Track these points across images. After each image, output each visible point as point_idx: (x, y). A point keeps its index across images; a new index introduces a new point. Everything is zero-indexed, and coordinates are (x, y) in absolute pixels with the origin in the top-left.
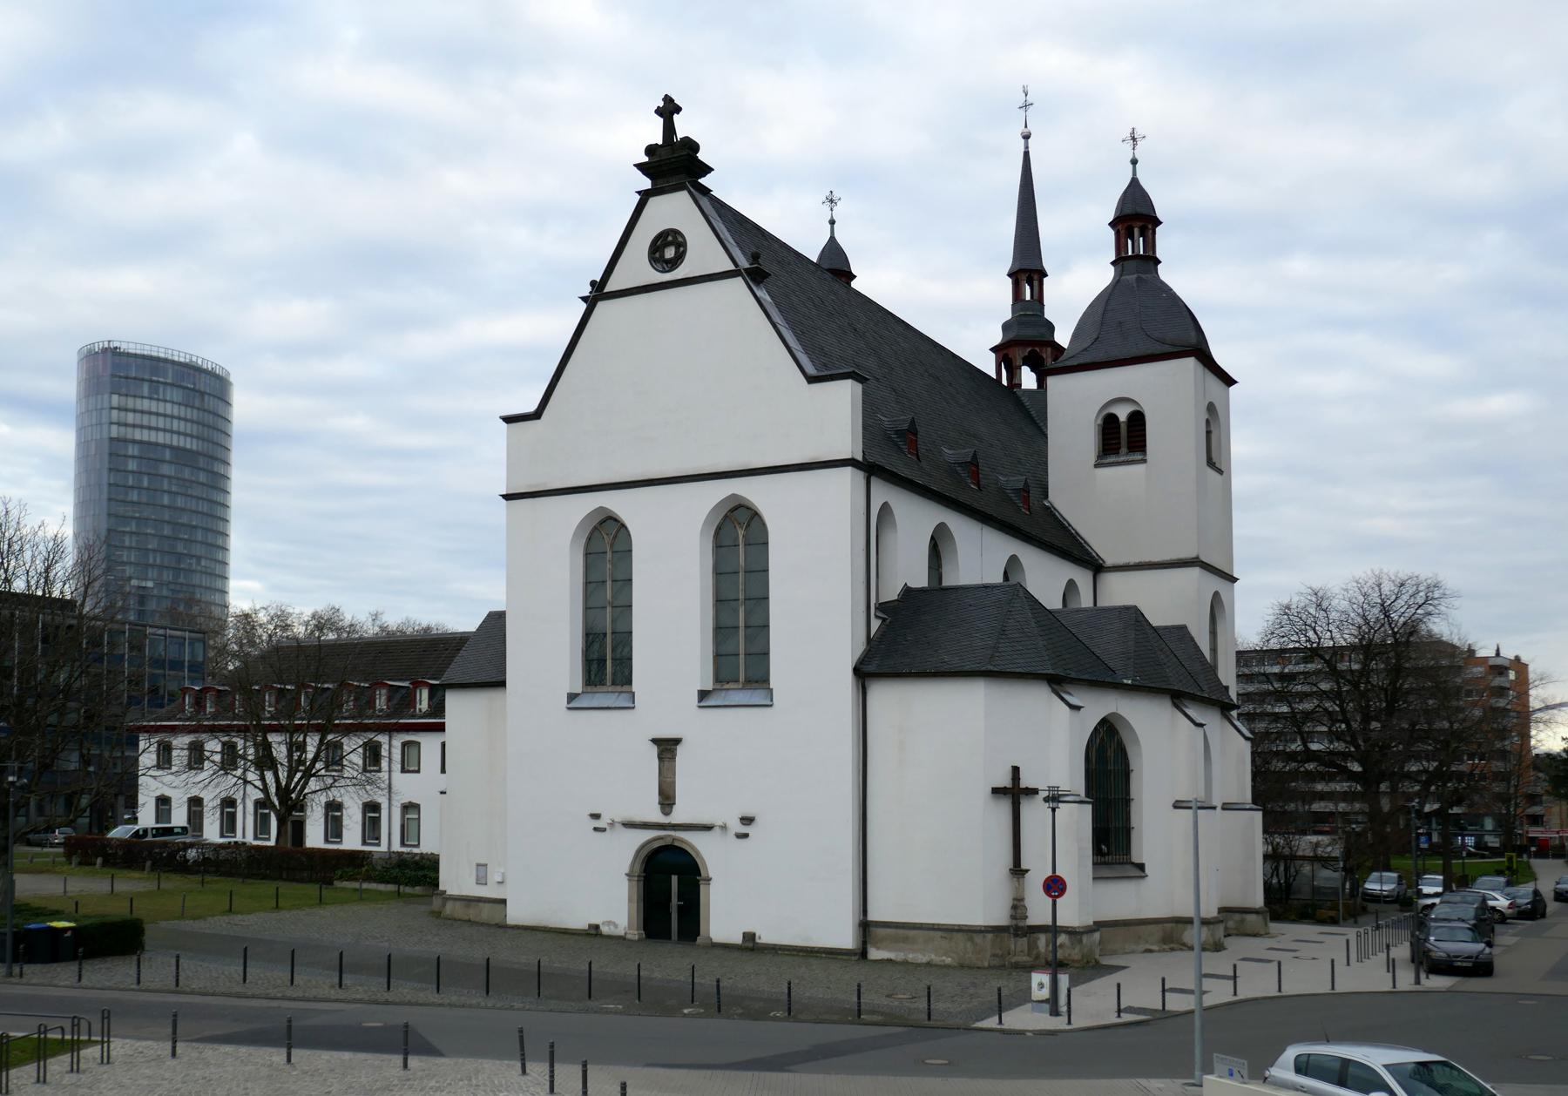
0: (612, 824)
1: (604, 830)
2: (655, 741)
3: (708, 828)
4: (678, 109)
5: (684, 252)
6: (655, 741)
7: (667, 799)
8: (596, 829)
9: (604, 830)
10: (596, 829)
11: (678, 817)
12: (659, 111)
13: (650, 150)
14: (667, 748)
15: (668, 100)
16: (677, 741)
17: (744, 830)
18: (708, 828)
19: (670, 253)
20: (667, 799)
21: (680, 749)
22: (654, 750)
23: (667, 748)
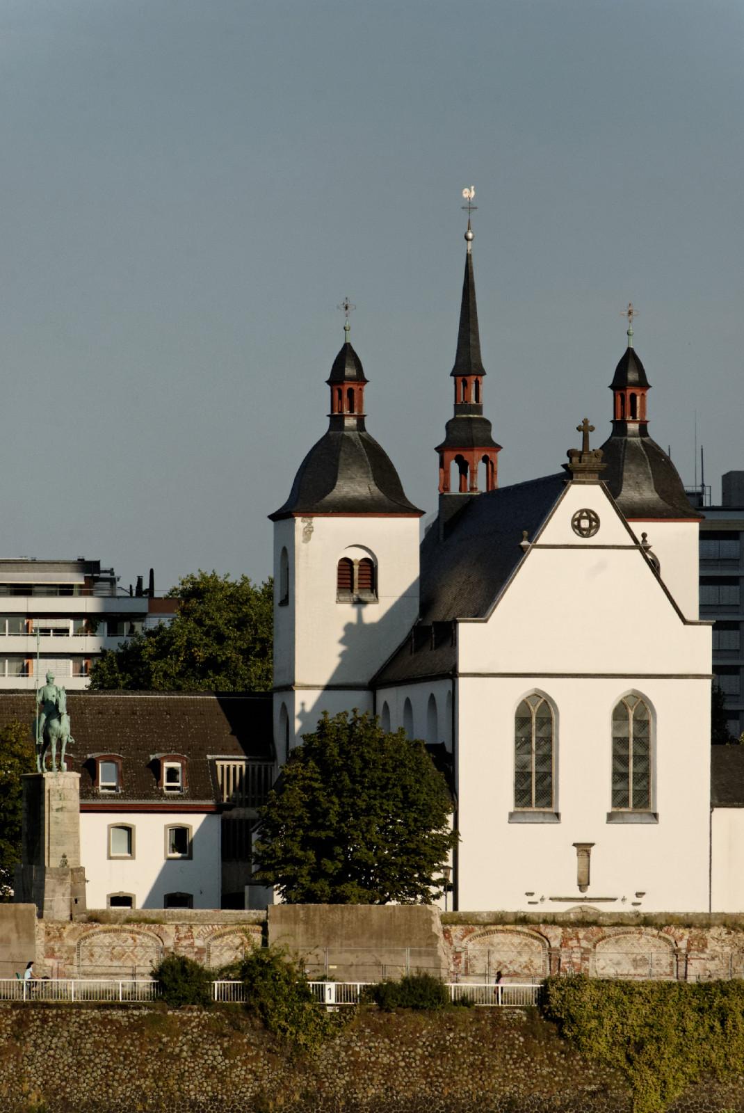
0: (542, 899)
1: (535, 903)
2: (575, 845)
3: (614, 900)
4: (592, 429)
5: (598, 526)
6: (575, 845)
7: (583, 884)
8: (530, 903)
9: (535, 903)
10: (530, 903)
11: (591, 892)
12: (579, 429)
13: (570, 454)
14: (584, 849)
15: (585, 422)
16: (592, 845)
17: (638, 900)
18: (614, 900)
19: (585, 524)
20: (583, 884)
21: (593, 849)
22: (575, 849)
23: (584, 849)
